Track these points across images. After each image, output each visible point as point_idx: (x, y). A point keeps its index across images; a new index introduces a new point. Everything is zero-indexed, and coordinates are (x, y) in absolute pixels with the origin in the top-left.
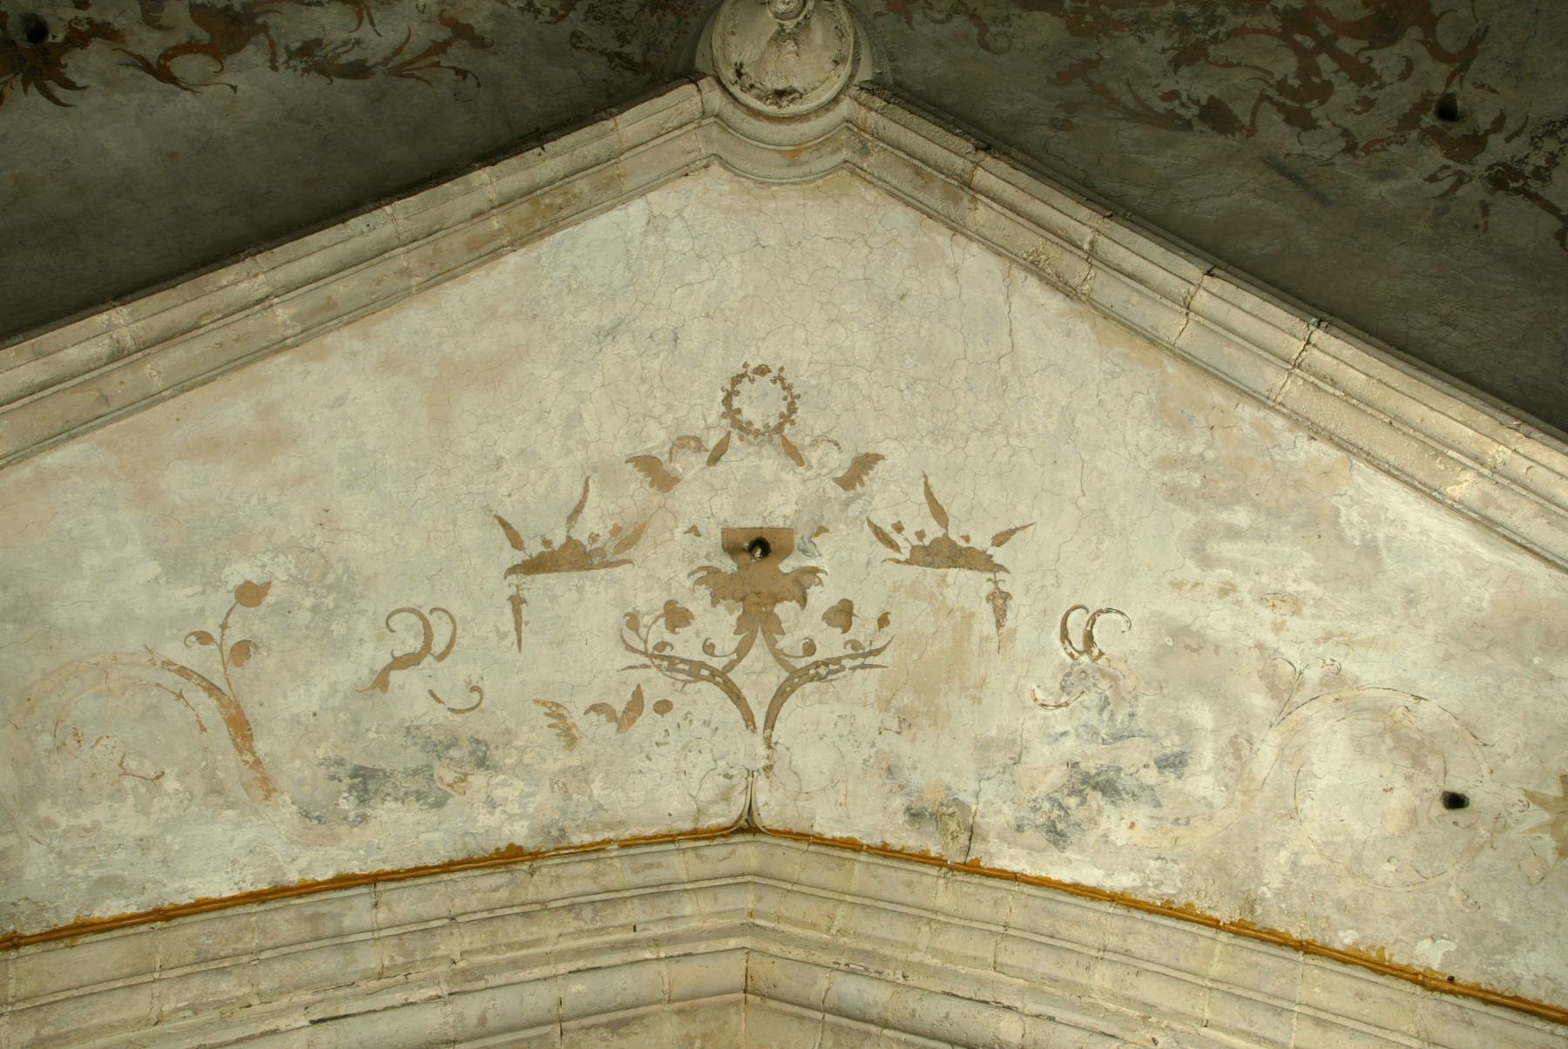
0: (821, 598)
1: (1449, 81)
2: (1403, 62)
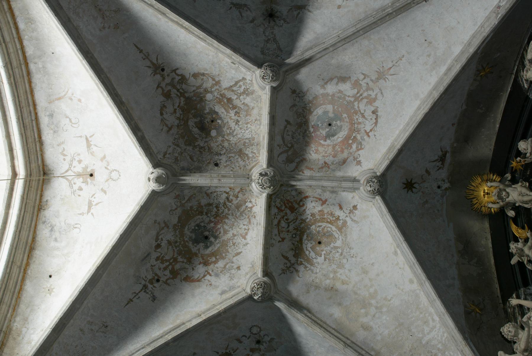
0: (83, 186)
1: (162, 281)
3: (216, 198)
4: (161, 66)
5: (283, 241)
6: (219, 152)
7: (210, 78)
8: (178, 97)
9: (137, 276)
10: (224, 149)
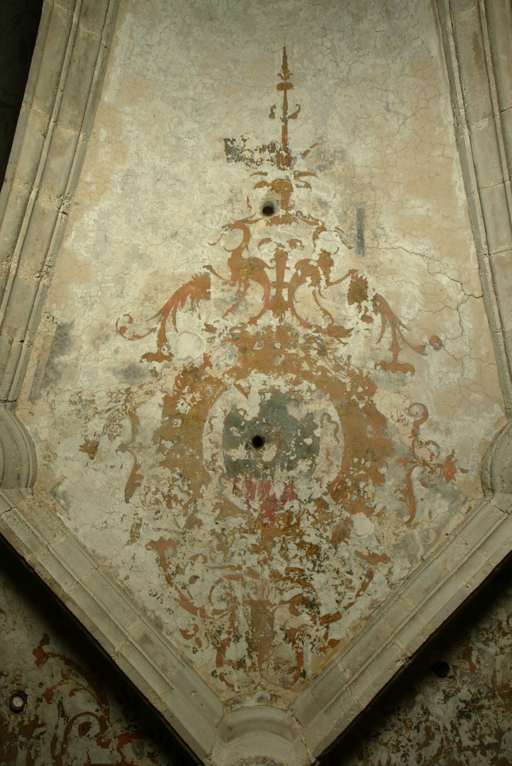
1: (256, 221)
2: (263, 246)
3: (342, 570)
5: (35, 652)
6: (475, 717)
9: (332, 163)
10: (471, 744)
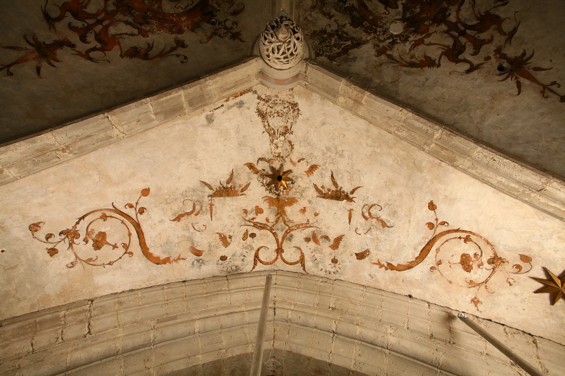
4: (506, 75)
7: (397, 59)
8: (462, 20)
